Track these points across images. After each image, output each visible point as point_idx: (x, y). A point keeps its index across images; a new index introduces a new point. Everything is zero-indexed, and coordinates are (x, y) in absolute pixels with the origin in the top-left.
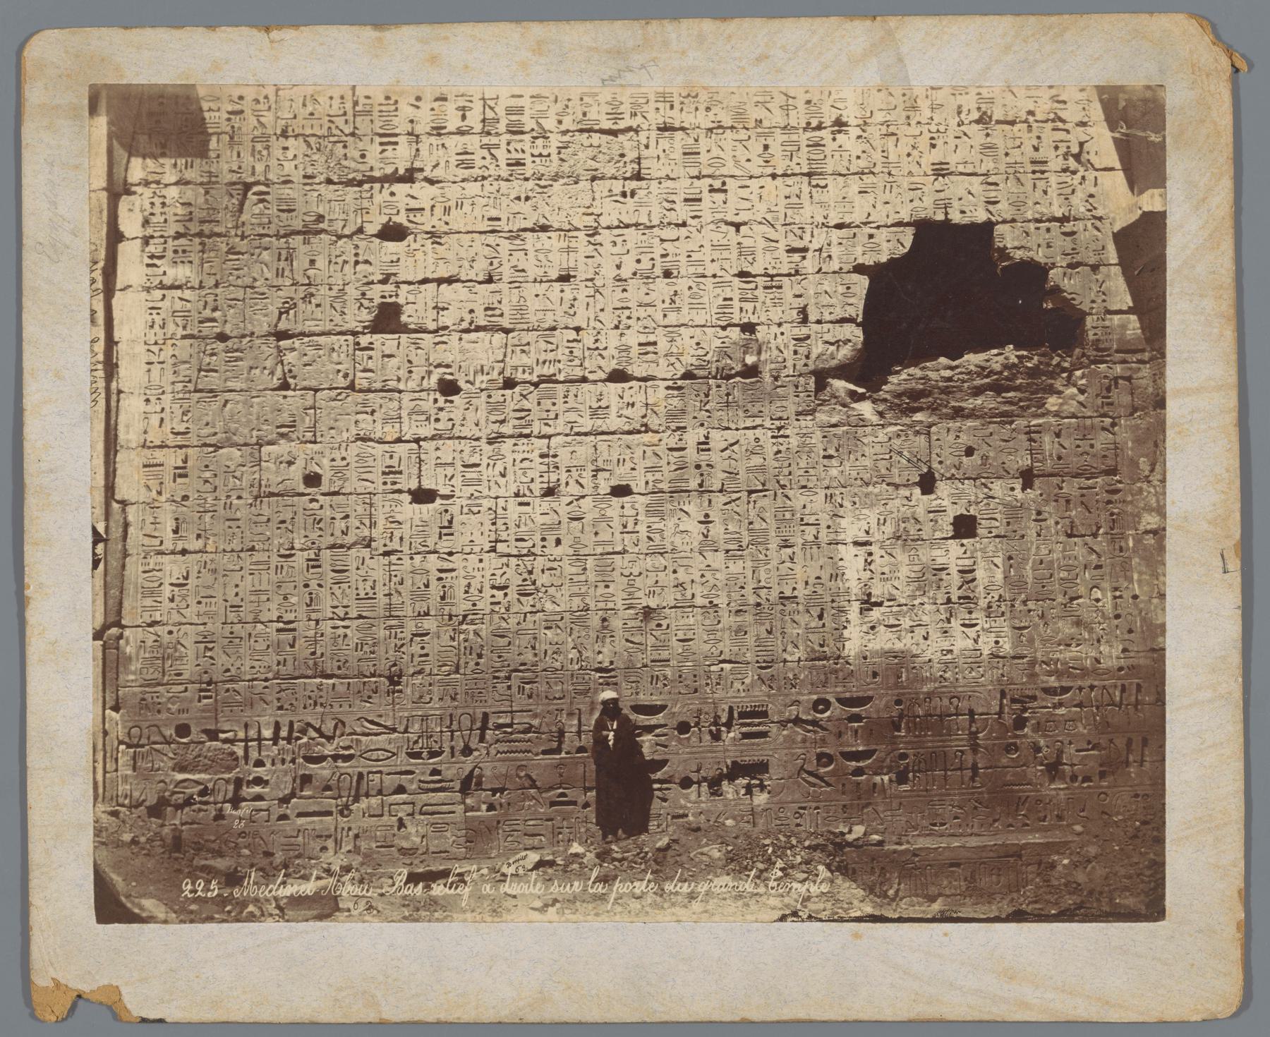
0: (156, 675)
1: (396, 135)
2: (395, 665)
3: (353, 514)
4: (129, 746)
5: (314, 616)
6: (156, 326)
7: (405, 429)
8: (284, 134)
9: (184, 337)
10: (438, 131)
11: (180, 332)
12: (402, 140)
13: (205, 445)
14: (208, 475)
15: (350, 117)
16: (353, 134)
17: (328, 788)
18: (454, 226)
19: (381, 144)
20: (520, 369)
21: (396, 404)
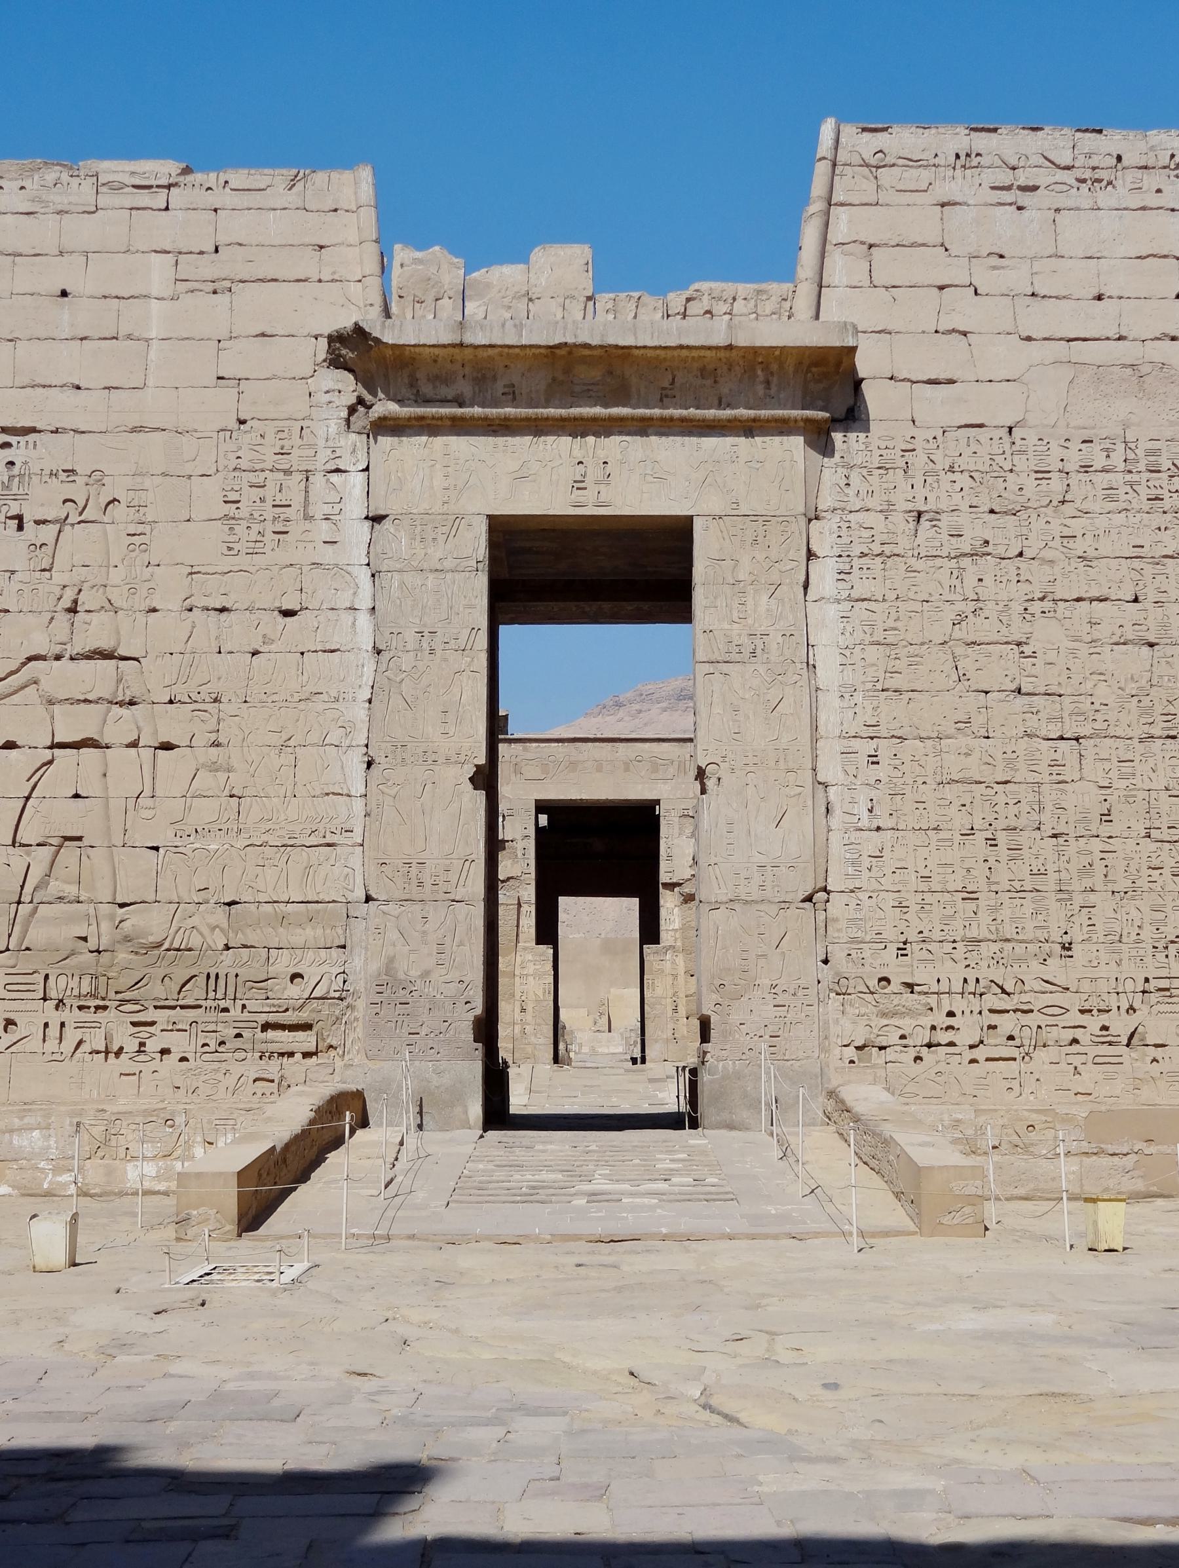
0: (859, 934)
1: (1049, 472)
2: (1066, 933)
3: (1024, 802)
4: (838, 994)
5: (994, 888)
6: (848, 634)
7: (1067, 727)
8: (951, 470)
9: (872, 644)
10: (1086, 468)
11: (868, 639)
12: (1055, 476)
13: (896, 737)
14: (898, 762)
15: (1008, 455)
16: (1011, 471)
17: (1011, 1038)
18: (1103, 552)
19: (1036, 479)
20: (1166, 678)
21: (1058, 706)
